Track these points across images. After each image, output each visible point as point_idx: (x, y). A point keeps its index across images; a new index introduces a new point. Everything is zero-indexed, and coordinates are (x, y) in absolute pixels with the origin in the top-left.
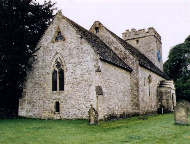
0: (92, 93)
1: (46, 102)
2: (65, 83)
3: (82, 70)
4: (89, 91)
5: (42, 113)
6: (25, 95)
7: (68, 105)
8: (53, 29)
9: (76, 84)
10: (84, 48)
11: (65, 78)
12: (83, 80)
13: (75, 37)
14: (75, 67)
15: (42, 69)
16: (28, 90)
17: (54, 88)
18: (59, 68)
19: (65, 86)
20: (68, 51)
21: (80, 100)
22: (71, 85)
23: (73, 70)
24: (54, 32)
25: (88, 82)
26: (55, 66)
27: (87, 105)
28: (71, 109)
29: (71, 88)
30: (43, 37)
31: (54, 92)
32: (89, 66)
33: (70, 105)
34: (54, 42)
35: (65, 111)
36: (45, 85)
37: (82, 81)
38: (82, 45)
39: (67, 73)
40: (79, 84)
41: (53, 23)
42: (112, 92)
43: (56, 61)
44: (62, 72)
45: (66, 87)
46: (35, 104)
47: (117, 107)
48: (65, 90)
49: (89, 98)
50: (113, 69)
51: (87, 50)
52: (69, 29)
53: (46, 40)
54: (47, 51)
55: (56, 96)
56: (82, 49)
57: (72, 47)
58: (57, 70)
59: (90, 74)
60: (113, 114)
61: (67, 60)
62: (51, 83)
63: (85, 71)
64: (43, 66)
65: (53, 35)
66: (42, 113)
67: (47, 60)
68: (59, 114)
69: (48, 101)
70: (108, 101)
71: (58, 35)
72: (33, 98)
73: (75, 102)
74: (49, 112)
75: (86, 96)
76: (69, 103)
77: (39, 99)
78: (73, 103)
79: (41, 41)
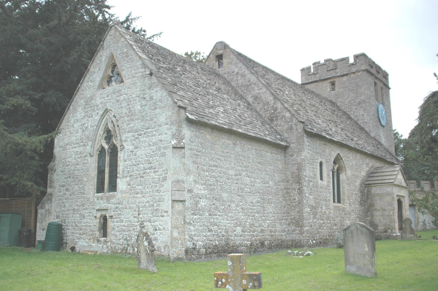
0: (166, 199)
1: (84, 217)
2: (118, 175)
3: (150, 145)
4: (161, 193)
5: (77, 240)
6: (51, 200)
7: (122, 224)
8: (104, 58)
9: (137, 177)
10: (155, 98)
11: (118, 165)
12: (150, 168)
13: (140, 74)
14: (137, 140)
15: (80, 146)
16: (56, 190)
17: (100, 189)
18: (112, 145)
19: (118, 180)
20: (126, 104)
21: (144, 212)
22: (128, 179)
23: (133, 147)
24: (103, 67)
25: (159, 173)
26: (104, 138)
27: (155, 224)
28: (127, 233)
29: (129, 187)
30: (86, 79)
31: (99, 194)
32: (163, 137)
33: (126, 224)
34: (104, 88)
35: (116, 236)
36: (85, 179)
37: (148, 171)
38: (151, 91)
39: (123, 152)
40: (143, 177)
41: (103, 48)
42: (225, 195)
43: (105, 127)
44: (114, 151)
45: (121, 184)
46: (67, 221)
47: (239, 229)
48: (117, 190)
49: (160, 208)
50: (230, 142)
51: (160, 101)
52: (130, 57)
53: (90, 83)
54: (91, 107)
55: (103, 204)
56: (151, 98)
57: (134, 96)
58: (106, 147)
59: (163, 155)
60: (227, 244)
61: (123, 123)
62: (94, 173)
63: (154, 148)
64: (82, 138)
65: (103, 72)
66: (77, 240)
67: (89, 127)
68: (105, 241)
69: (88, 214)
70: (210, 215)
71: (112, 72)
72: (65, 206)
73: (135, 217)
74: (89, 238)
75: (155, 205)
76: (124, 220)
77: (74, 209)
78: (132, 218)
79: (82, 88)
